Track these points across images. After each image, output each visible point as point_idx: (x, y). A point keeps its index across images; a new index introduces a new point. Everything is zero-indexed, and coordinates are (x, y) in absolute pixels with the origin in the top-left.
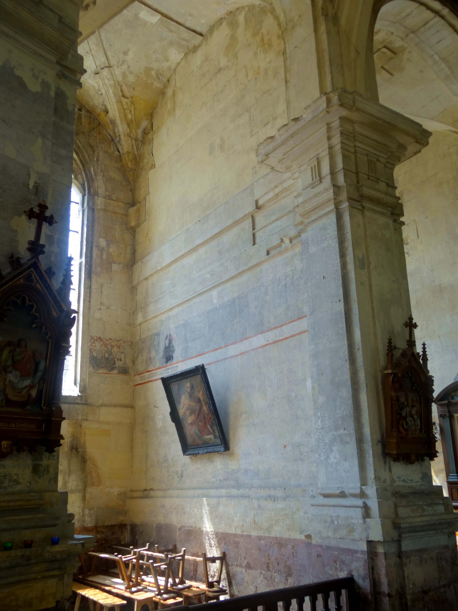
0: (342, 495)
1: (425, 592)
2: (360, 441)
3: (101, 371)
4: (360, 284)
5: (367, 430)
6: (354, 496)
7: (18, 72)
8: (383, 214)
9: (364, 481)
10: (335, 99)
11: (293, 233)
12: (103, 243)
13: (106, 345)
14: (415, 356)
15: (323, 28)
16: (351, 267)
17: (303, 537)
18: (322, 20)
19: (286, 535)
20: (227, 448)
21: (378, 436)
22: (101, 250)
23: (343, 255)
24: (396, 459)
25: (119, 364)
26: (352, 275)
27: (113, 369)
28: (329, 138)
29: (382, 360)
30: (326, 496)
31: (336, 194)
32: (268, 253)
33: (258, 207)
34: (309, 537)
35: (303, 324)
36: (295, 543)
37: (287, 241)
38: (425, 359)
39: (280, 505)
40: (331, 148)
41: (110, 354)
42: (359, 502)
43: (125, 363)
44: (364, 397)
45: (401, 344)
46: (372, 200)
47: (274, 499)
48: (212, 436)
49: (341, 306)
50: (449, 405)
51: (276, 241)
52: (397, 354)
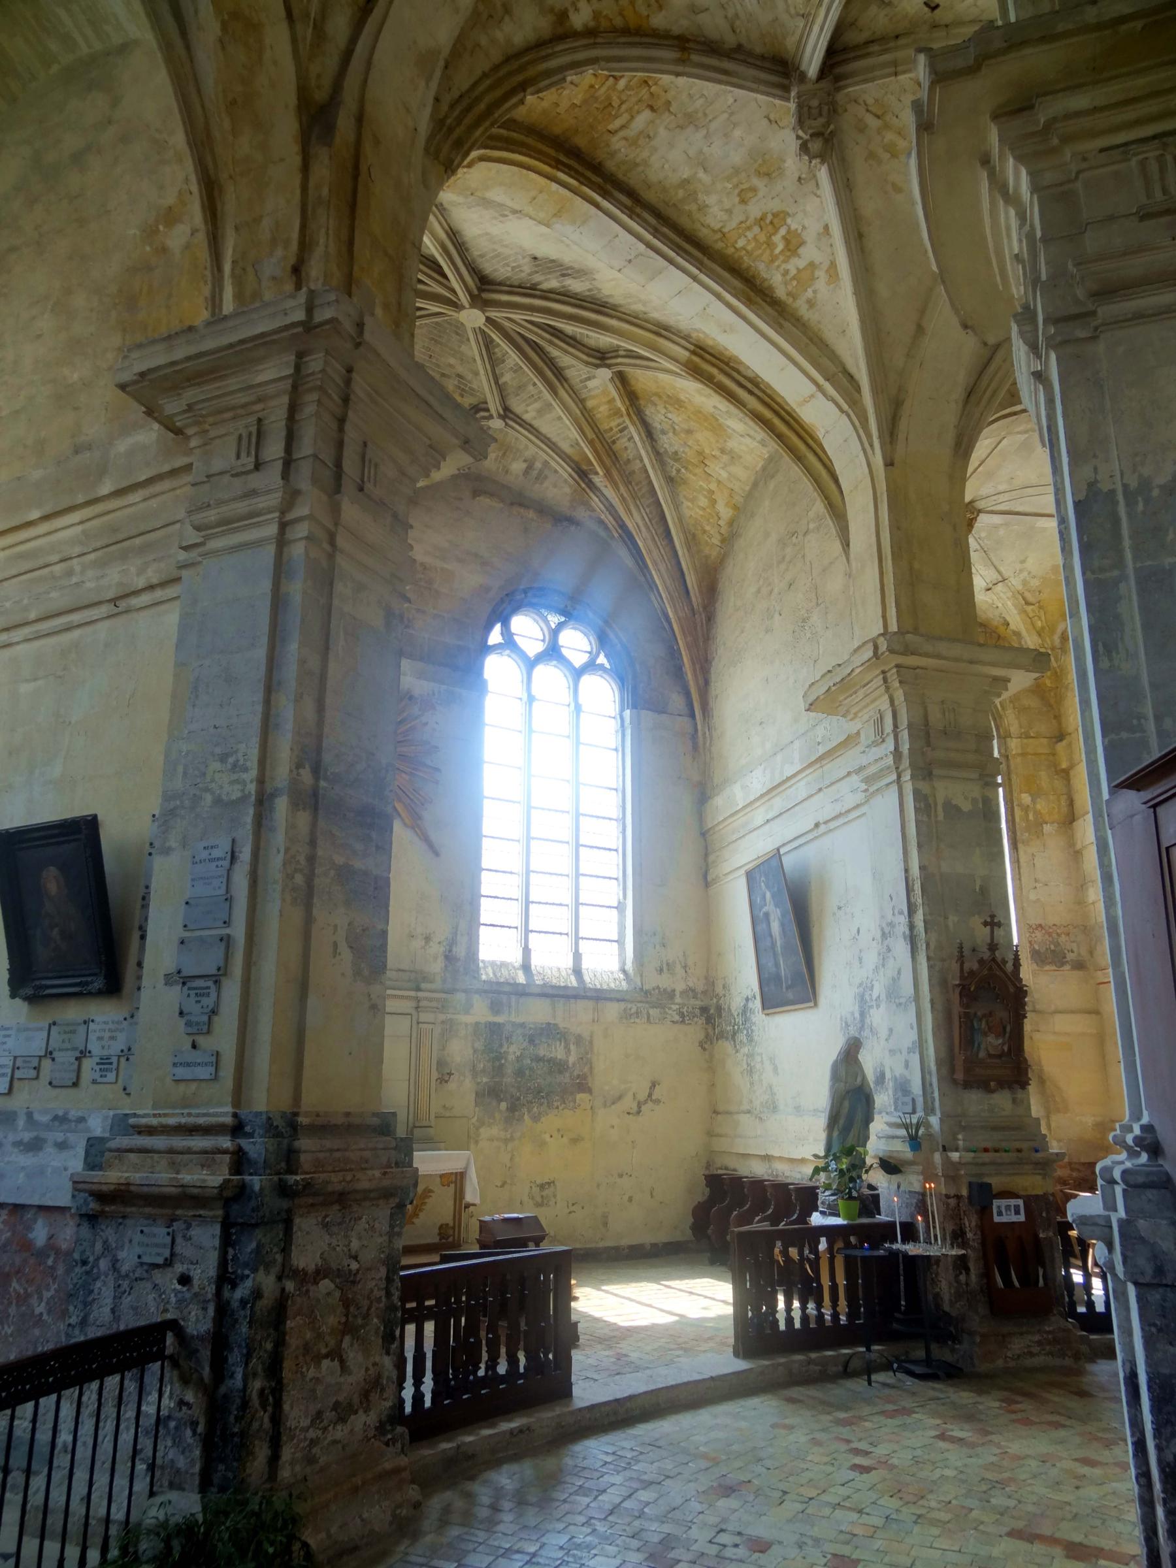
3: (1047, 968)
7: (954, 802)
12: (1026, 798)
13: (1050, 934)
22: (1026, 809)
25: (1070, 956)
27: (1063, 964)
41: (1057, 944)
43: (1079, 954)
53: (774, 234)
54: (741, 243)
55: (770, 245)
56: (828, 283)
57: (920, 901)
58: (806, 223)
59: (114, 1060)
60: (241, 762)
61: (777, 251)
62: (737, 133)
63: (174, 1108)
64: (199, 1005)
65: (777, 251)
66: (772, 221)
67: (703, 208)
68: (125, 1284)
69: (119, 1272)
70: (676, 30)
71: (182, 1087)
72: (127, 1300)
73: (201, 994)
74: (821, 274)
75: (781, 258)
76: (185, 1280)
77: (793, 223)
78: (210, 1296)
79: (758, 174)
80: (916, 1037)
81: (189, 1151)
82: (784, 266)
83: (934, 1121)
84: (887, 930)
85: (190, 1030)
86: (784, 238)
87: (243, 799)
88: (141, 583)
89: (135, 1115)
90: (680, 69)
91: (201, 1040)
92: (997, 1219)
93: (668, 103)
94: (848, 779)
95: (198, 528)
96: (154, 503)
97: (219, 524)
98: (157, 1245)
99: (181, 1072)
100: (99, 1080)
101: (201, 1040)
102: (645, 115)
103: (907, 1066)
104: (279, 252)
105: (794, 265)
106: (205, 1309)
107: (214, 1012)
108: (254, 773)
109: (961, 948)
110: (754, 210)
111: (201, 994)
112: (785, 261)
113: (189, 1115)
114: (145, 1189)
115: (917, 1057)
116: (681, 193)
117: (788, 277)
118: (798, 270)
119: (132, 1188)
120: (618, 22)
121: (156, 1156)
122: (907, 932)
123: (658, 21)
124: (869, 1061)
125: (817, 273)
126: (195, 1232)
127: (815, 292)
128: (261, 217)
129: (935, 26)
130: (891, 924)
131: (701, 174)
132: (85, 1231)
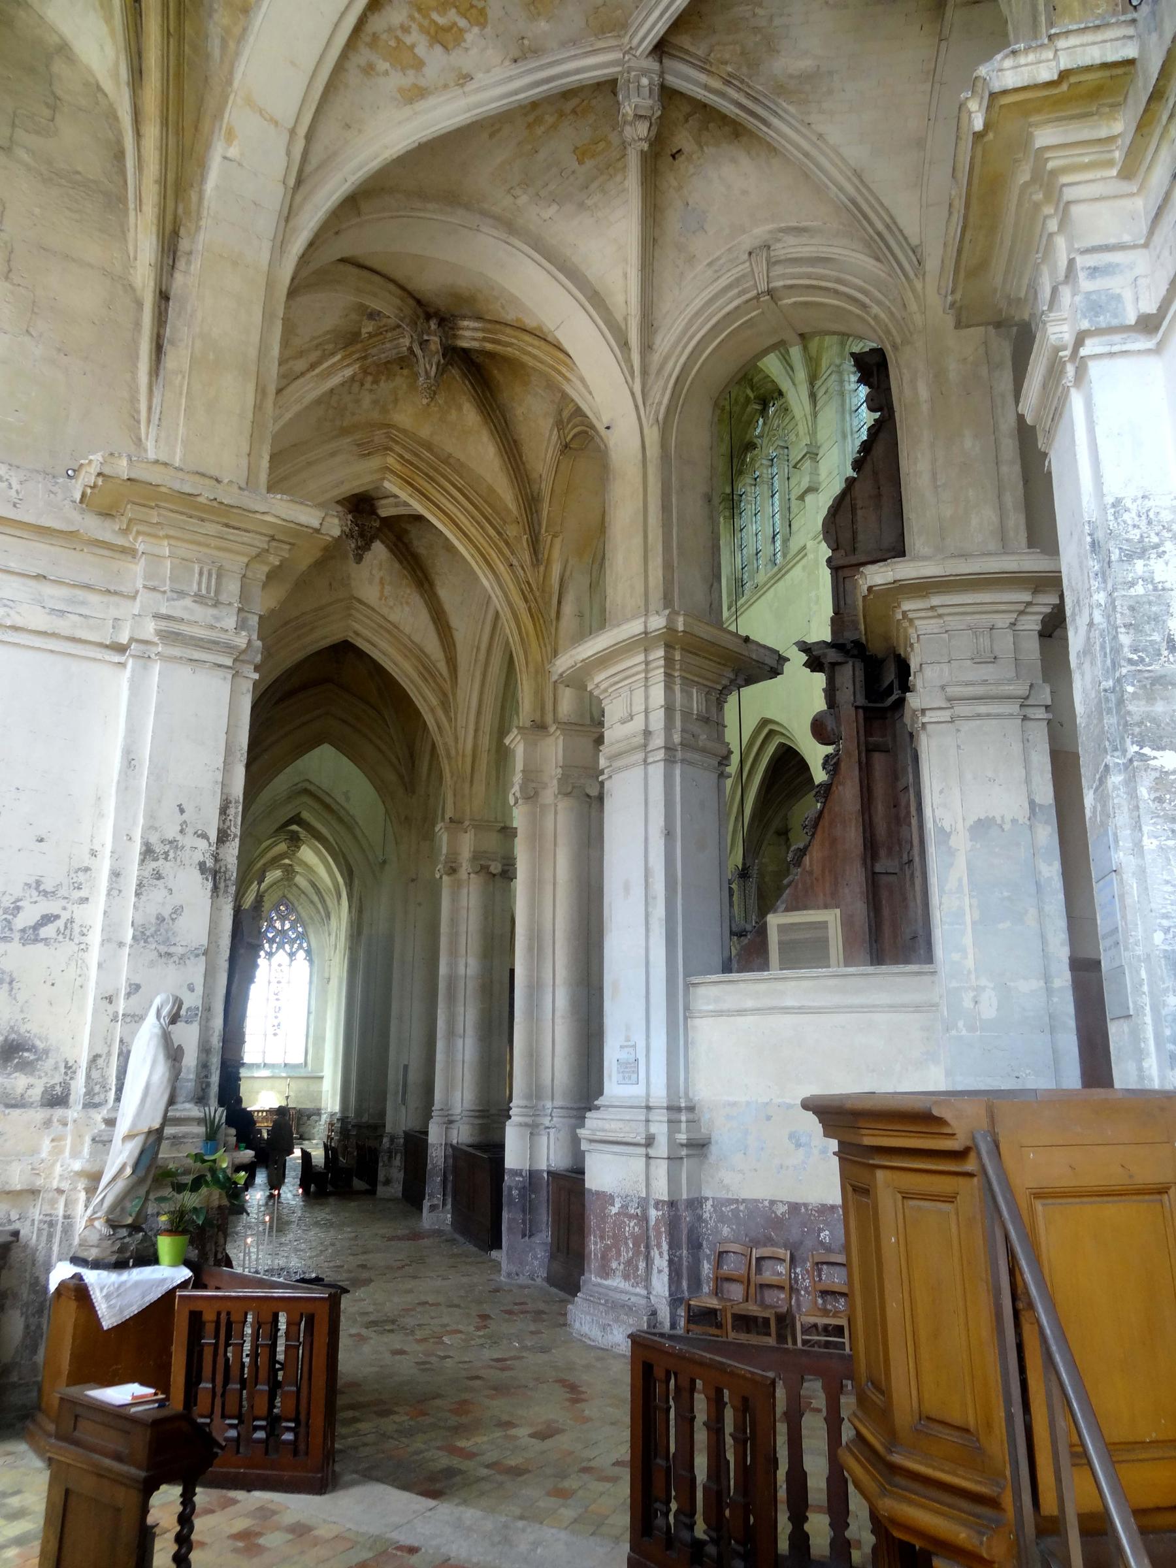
53: (459, 12)
56: (401, 90)
57: (236, 830)
58: (474, 52)
61: (435, 16)
65: (435, 16)
74: (408, 79)
75: (426, 23)
82: (414, 27)
84: (159, 848)
86: (455, 24)
94: (32, 583)
112: (421, 26)
117: (399, 33)
118: (413, 46)
125: (411, 72)
127: (386, 73)
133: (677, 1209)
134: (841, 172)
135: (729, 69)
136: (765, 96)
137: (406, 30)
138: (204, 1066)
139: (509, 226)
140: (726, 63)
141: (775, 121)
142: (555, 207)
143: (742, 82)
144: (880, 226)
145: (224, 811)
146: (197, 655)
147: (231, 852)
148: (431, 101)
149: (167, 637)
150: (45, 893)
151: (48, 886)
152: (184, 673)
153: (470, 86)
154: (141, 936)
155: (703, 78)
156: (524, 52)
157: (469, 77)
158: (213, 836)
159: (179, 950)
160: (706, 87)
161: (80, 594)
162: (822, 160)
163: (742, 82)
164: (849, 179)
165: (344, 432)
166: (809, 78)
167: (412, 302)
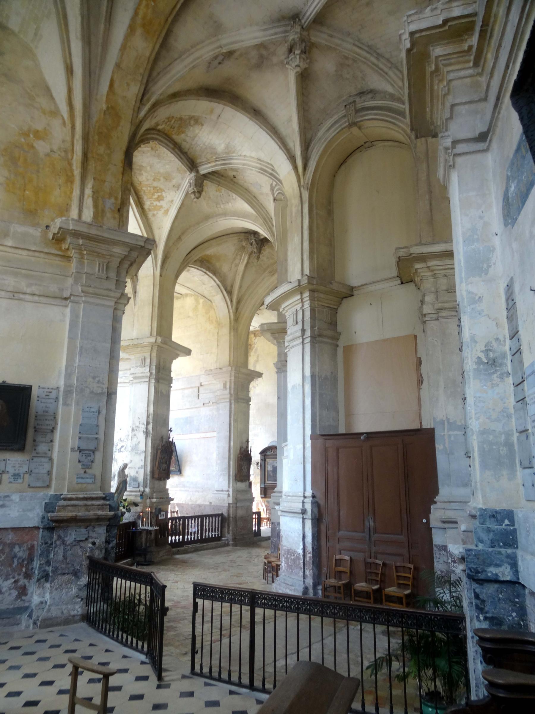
0: (222, 491)
1: (242, 517)
2: (229, 475)
4: (234, 427)
5: (231, 472)
6: (226, 491)
8: (244, 403)
9: (229, 487)
10: (234, 369)
11: (214, 401)
14: (248, 451)
15: (232, 334)
16: (232, 422)
17: (209, 503)
18: (232, 330)
19: (202, 503)
20: (181, 473)
21: (234, 474)
23: (230, 417)
24: (239, 481)
26: (232, 424)
28: (230, 377)
29: (238, 452)
30: (217, 491)
31: (231, 397)
32: (204, 404)
33: (201, 385)
34: (211, 503)
35: (215, 434)
36: (205, 506)
37: (211, 403)
38: (251, 451)
39: (201, 494)
40: (230, 380)
42: (227, 493)
44: (231, 463)
45: (245, 447)
46: (241, 399)
47: (199, 492)
48: (174, 468)
49: (228, 434)
50: (265, 455)
51: (207, 402)
52: (243, 450)
54: (144, 188)
55: (153, 194)
56: (163, 214)
57: (151, 421)
58: (168, 196)
59: (22, 475)
60: (101, 381)
61: (154, 197)
62: (167, 166)
63: (76, 492)
64: (86, 460)
66: (157, 190)
67: (141, 174)
68: (69, 548)
69: (66, 544)
70: (176, 140)
71: (80, 485)
72: (69, 553)
73: (87, 456)
74: (163, 210)
76: (94, 544)
77: (164, 194)
78: (103, 547)
79: (164, 177)
80: (144, 464)
81: (93, 505)
83: (148, 490)
84: (135, 429)
85: (83, 467)
86: (159, 196)
87: (102, 394)
88: (29, 291)
89: (62, 494)
90: (172, 151)
91: (88, 470)
92: (160, 518)
93: (157, 150)
95: (83, 292)
96: (33, 259)
97: (92, 294)
98: (82, 534)
99: (80, 480)
100: (13, 482)
101: (88, 470)
102: (150, 149)
103: (137, 472)
104: (113, 200)
105: (155, 203)
106: (101, 551)
107: (93, 462)
108: (106, 386)
109: (162, 438)
110: (155, 184)
111: (87, 456)
113: (86, 494)
114: (83, 517)
115: (143, 470)
116: (138, 167)
119: (78, 518)
120: (166, 132)
121: (80, 507)
122: (145, 430)
123: (174, 137)
124: (127, 471)
126: (97, 529)
128: (105, 181)
129: (232, 180)
130: (137, 427)
131: (148, 168)
132: (46, 533)
133: (275, 525)
134: (255, 162)
135: (214, 157)
136: (226, 157)
137: (152, 203)
138: (145, 479)
139: (225, 214)
140: (212, 157)
141: (232, 161)
142: (230, 203)
143: (219, 158)
144: (271, 171)
145: (148, 417)
146: (141, 380)
147: (150, 427)
148: (170, 211)
149: (135, 378)
150: (122, 441)
151: (122, 439)
152: (139, 385)
153: (174, 202)
154: (132, 449)
155: (209, 165)
156: (177, 187)
157: (172, 201)
158: (145, 424)
159: (139, 452)
160: (212, 167)
161: (125, 371)
162: (249, 163)
163: (219, 158)
164: (257, 163)
165: (265, 270)
166: (227, 147)
167: (243, 234)
